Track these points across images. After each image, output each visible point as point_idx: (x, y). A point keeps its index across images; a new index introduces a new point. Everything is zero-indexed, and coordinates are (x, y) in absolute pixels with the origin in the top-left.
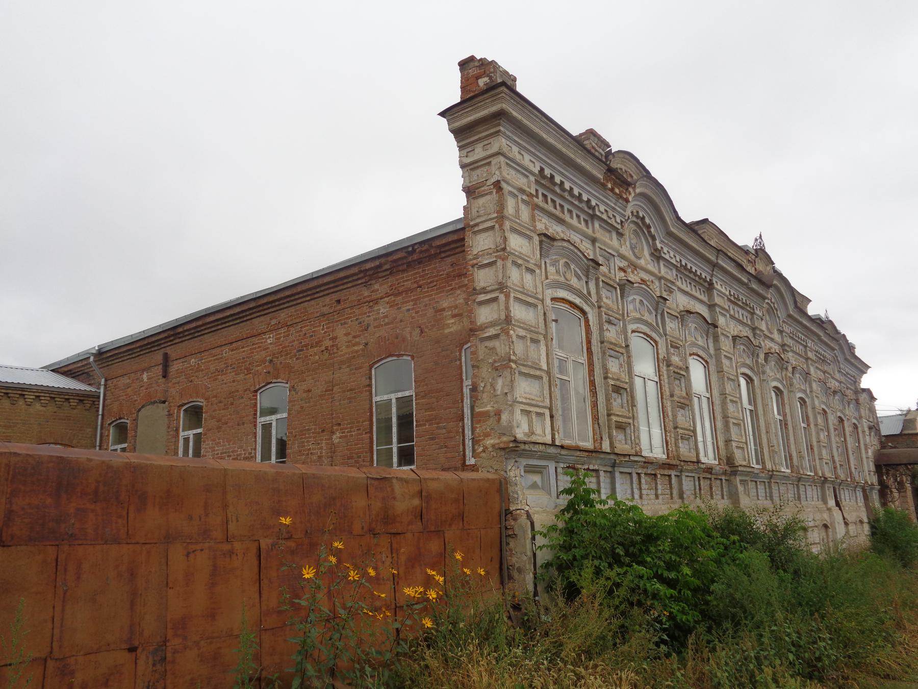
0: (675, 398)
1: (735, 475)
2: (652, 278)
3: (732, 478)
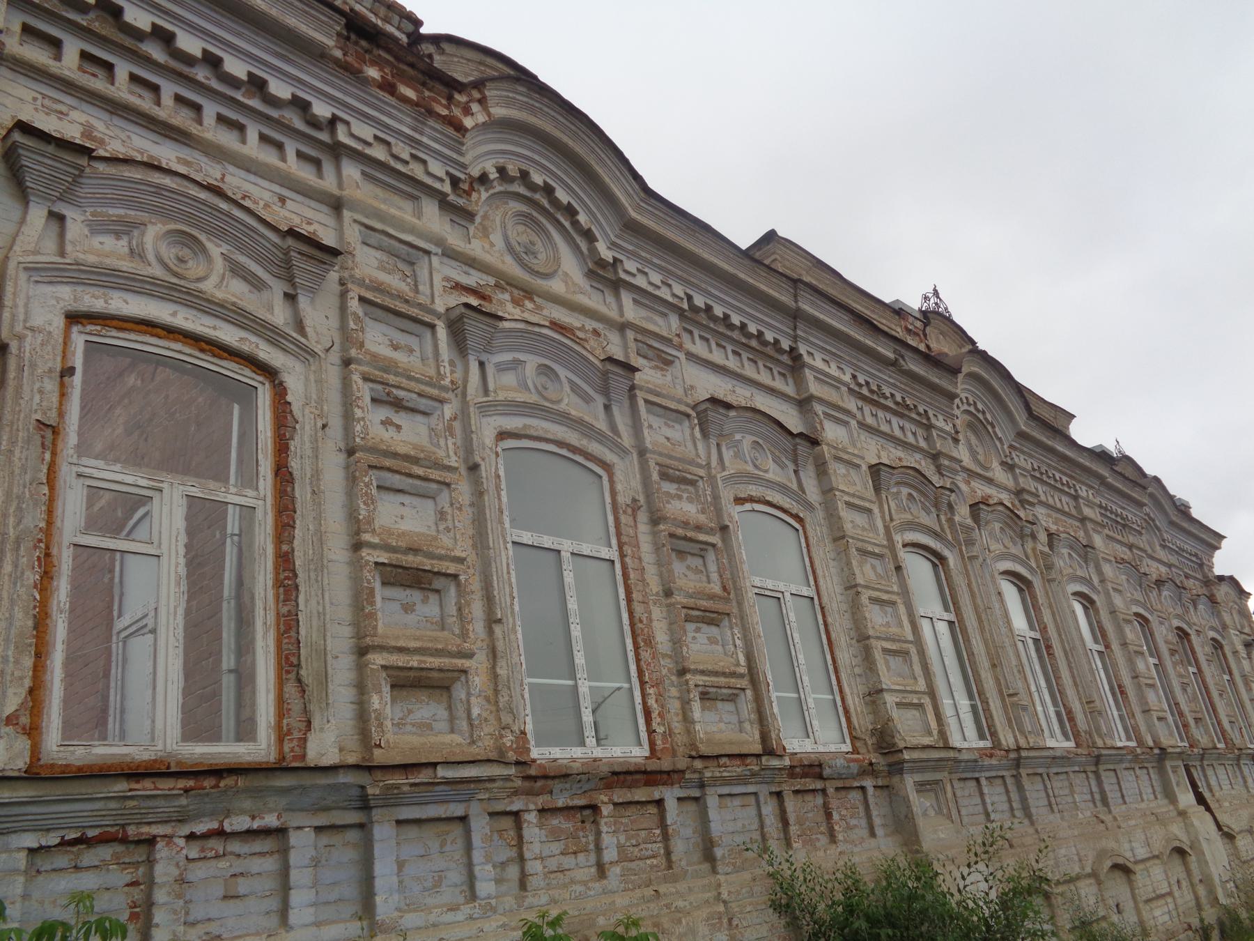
0: (679, 598)
1: (901, 772)
2: (590, 324)
3: (896, 780)
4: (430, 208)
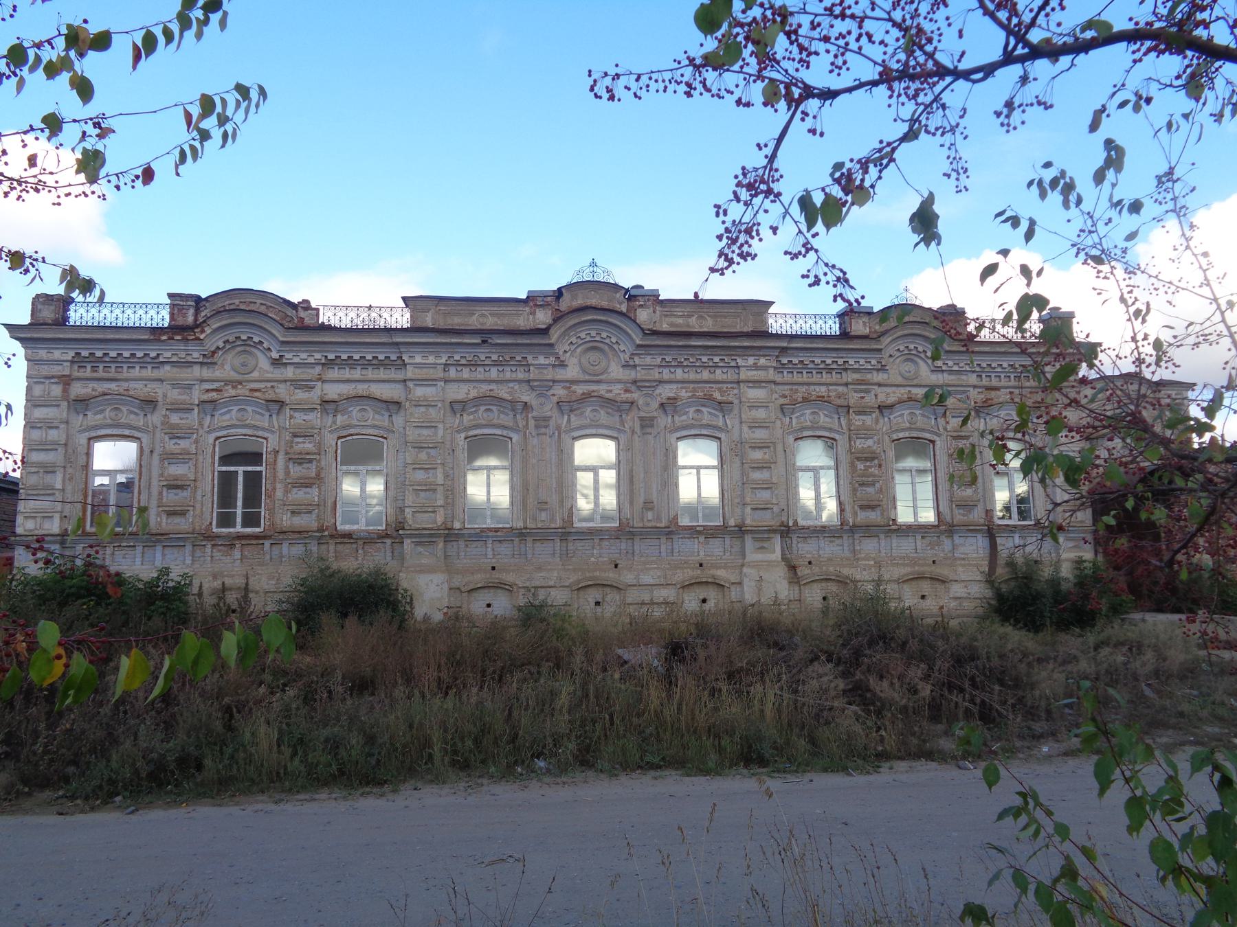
2: (269, 385)
4: (197, 368)
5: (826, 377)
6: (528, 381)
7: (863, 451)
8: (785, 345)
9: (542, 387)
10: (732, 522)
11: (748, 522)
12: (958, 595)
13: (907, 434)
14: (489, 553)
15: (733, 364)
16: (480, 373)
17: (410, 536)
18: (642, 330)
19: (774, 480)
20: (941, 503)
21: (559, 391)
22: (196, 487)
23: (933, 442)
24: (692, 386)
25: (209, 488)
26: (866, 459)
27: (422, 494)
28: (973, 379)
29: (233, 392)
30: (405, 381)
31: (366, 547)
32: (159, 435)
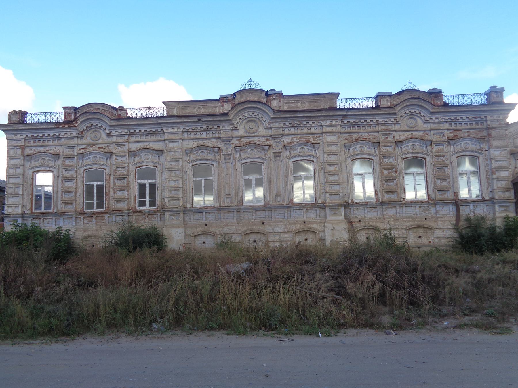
4: (76, 139)
5: (367, 129)
6: (221, 138)
7: (387, 164)
8: (345, 113)
9: (227, 140)
10: (320, 202)
11: (328, 201)
12: (439, 236)
13: (411, 155)
14: (203, 219)
15: (319, 124)
16: (198, 135)
17: (168, 211)
18: (273, 110)
19: (341, 180)
20: (429, 189)
21: (235, 142)
22: (76, 192)
23: (425, 159)
24: (299, 136)
25: (82, 191)
26: (389, 169)
27: (173, 192)
28: (447, 126)
29: (91, 149)
30: (164, 140)
31: (149, 216)
32: (61, 169)
